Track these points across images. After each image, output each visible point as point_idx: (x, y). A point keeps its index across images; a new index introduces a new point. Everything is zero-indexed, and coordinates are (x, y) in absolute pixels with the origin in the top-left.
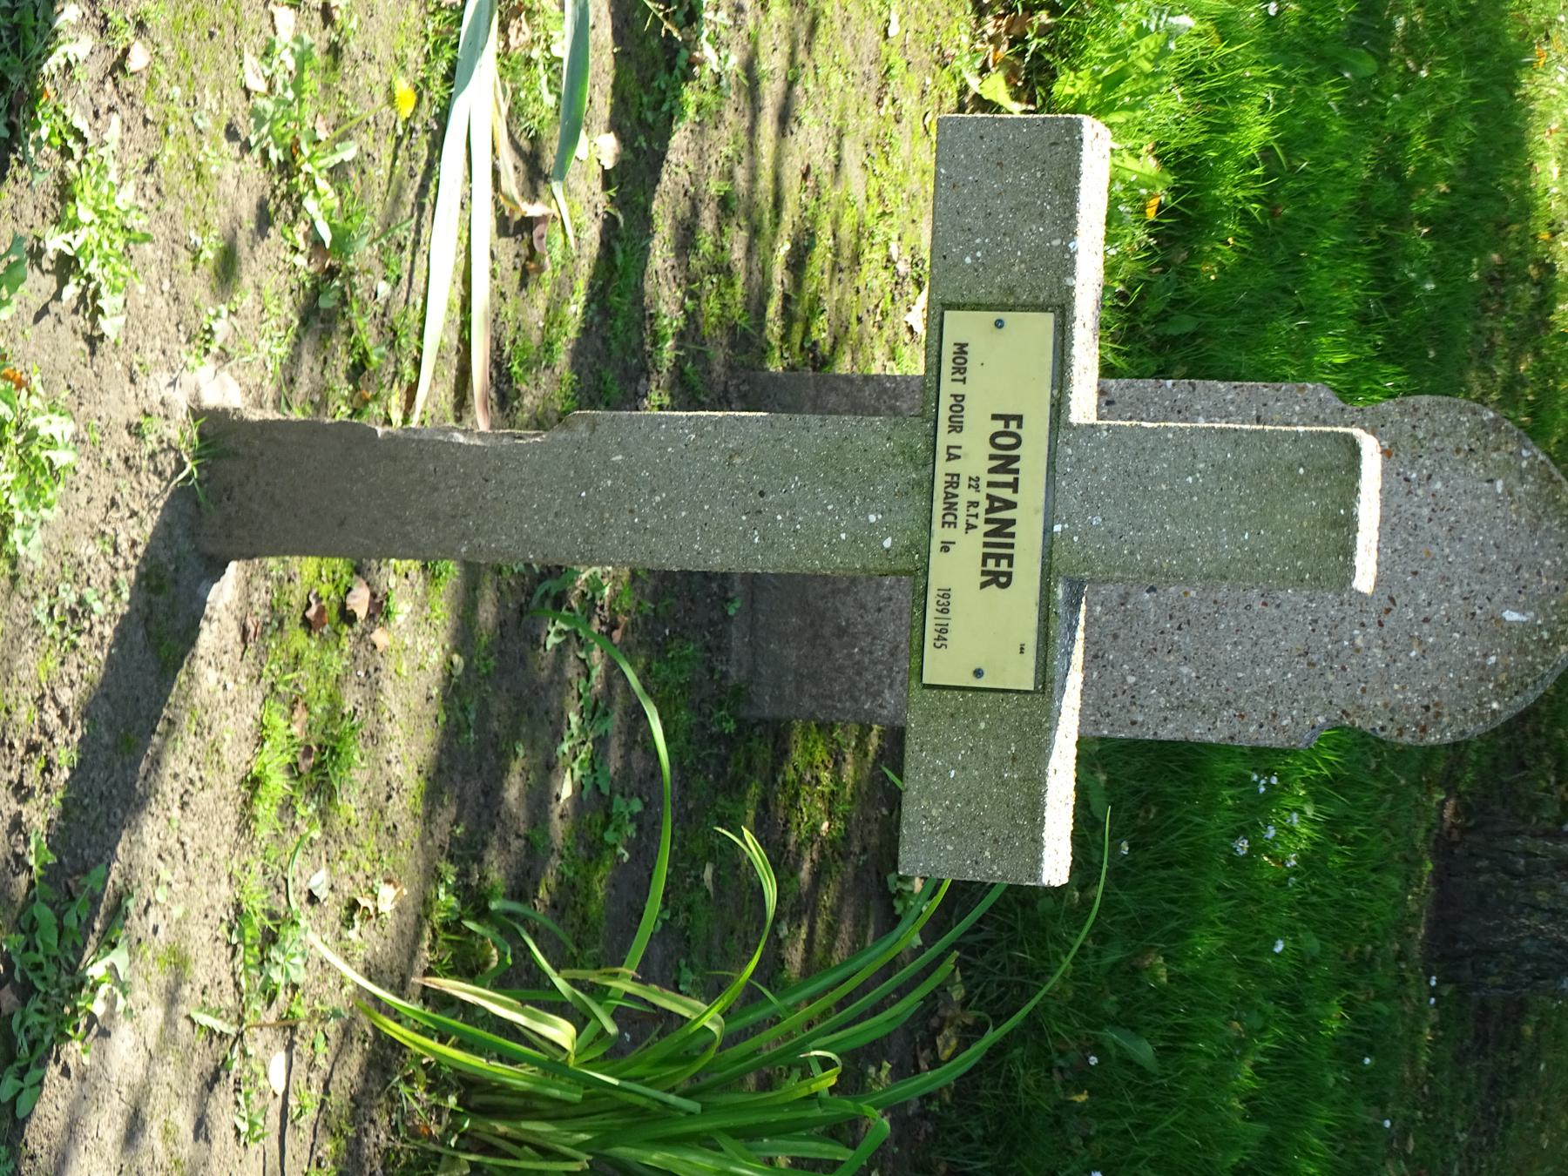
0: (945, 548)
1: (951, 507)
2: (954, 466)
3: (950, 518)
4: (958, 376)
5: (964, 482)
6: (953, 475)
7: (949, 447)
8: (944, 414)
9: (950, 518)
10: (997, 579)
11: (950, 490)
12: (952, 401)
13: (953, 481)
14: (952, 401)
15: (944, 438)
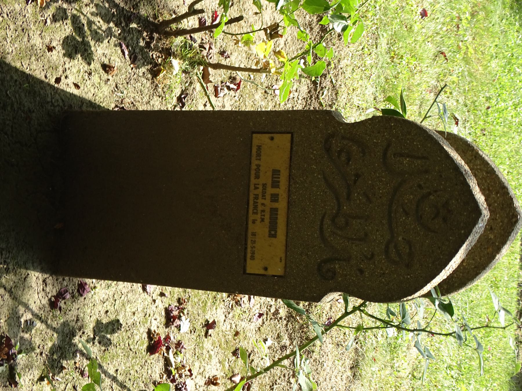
0: (254, 222)
1: (256, 207)
2: (256, 192)
3: (255, 211)
4: (259, 158)
5: (260, 196)
6: (256, 195)
7: (255, 184)
8: (253, 172)
9: (255, 211)
10: (273, 235)
11: (255, 200)
12: (256, 167)
13: (256, 197)
14: (256, 167)
15: (253, 181)
